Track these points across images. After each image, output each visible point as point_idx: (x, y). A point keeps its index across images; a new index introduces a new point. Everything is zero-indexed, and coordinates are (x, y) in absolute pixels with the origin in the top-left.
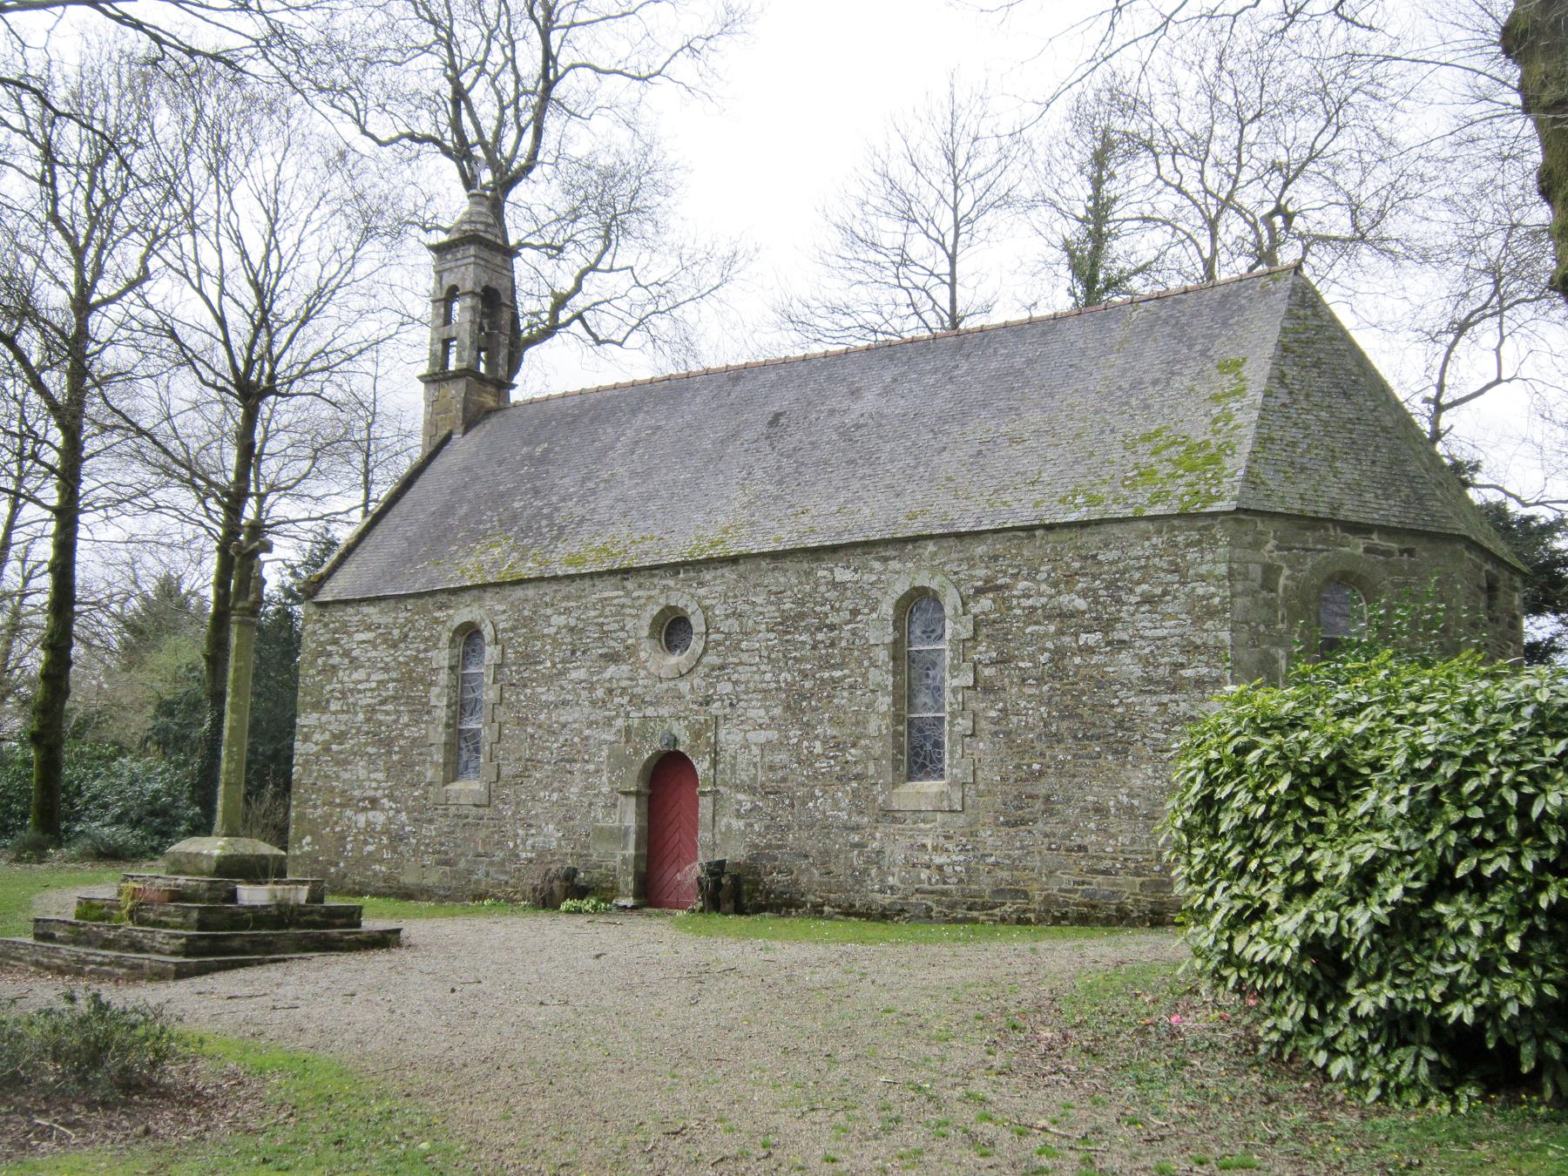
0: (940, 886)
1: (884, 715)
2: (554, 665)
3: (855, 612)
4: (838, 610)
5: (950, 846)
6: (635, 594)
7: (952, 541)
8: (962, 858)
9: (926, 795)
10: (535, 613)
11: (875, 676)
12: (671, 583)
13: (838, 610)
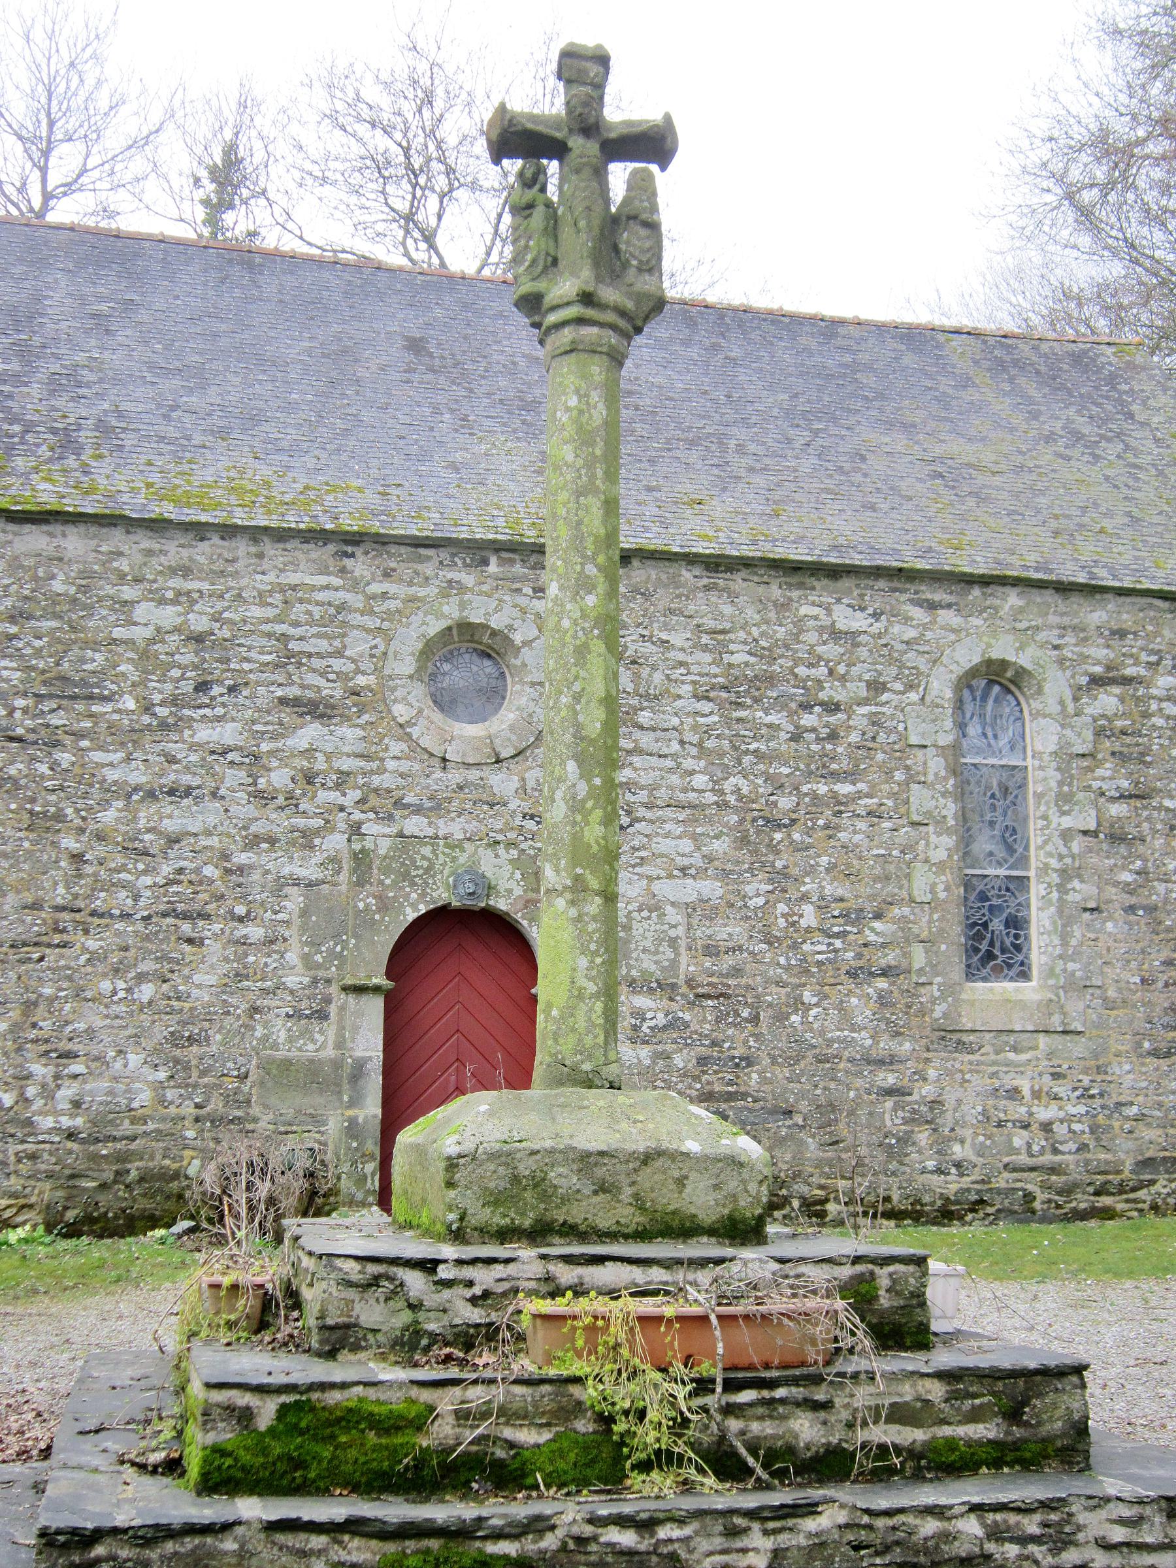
0: (1048, 1159)
1: (941, 866)
2: (148, 708)
3: (877, 687)
4: (843, 679)
5: (1061, 1089)
6: (376, 588)
7: (1049, 596)
8: (1082, 1109)
9: (1022, 1005)
10: (85, 589)
11: (921, 799)
12: (468, 579)
13: (843, 679)
